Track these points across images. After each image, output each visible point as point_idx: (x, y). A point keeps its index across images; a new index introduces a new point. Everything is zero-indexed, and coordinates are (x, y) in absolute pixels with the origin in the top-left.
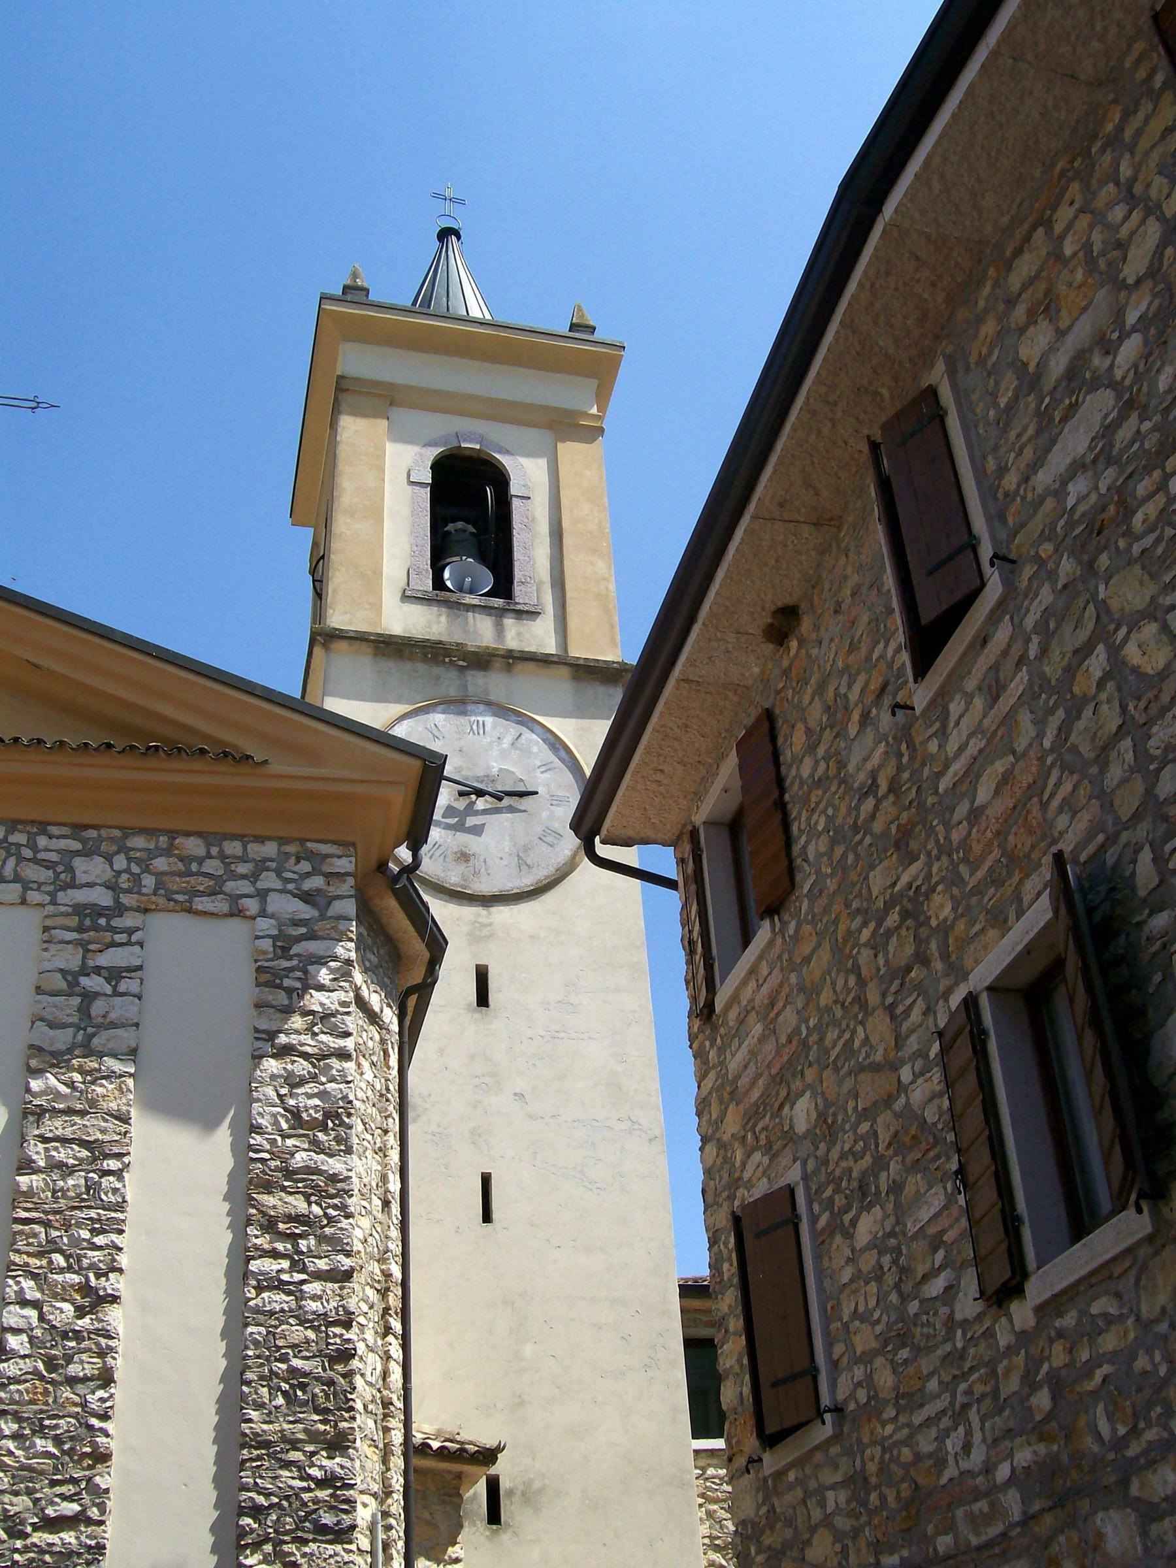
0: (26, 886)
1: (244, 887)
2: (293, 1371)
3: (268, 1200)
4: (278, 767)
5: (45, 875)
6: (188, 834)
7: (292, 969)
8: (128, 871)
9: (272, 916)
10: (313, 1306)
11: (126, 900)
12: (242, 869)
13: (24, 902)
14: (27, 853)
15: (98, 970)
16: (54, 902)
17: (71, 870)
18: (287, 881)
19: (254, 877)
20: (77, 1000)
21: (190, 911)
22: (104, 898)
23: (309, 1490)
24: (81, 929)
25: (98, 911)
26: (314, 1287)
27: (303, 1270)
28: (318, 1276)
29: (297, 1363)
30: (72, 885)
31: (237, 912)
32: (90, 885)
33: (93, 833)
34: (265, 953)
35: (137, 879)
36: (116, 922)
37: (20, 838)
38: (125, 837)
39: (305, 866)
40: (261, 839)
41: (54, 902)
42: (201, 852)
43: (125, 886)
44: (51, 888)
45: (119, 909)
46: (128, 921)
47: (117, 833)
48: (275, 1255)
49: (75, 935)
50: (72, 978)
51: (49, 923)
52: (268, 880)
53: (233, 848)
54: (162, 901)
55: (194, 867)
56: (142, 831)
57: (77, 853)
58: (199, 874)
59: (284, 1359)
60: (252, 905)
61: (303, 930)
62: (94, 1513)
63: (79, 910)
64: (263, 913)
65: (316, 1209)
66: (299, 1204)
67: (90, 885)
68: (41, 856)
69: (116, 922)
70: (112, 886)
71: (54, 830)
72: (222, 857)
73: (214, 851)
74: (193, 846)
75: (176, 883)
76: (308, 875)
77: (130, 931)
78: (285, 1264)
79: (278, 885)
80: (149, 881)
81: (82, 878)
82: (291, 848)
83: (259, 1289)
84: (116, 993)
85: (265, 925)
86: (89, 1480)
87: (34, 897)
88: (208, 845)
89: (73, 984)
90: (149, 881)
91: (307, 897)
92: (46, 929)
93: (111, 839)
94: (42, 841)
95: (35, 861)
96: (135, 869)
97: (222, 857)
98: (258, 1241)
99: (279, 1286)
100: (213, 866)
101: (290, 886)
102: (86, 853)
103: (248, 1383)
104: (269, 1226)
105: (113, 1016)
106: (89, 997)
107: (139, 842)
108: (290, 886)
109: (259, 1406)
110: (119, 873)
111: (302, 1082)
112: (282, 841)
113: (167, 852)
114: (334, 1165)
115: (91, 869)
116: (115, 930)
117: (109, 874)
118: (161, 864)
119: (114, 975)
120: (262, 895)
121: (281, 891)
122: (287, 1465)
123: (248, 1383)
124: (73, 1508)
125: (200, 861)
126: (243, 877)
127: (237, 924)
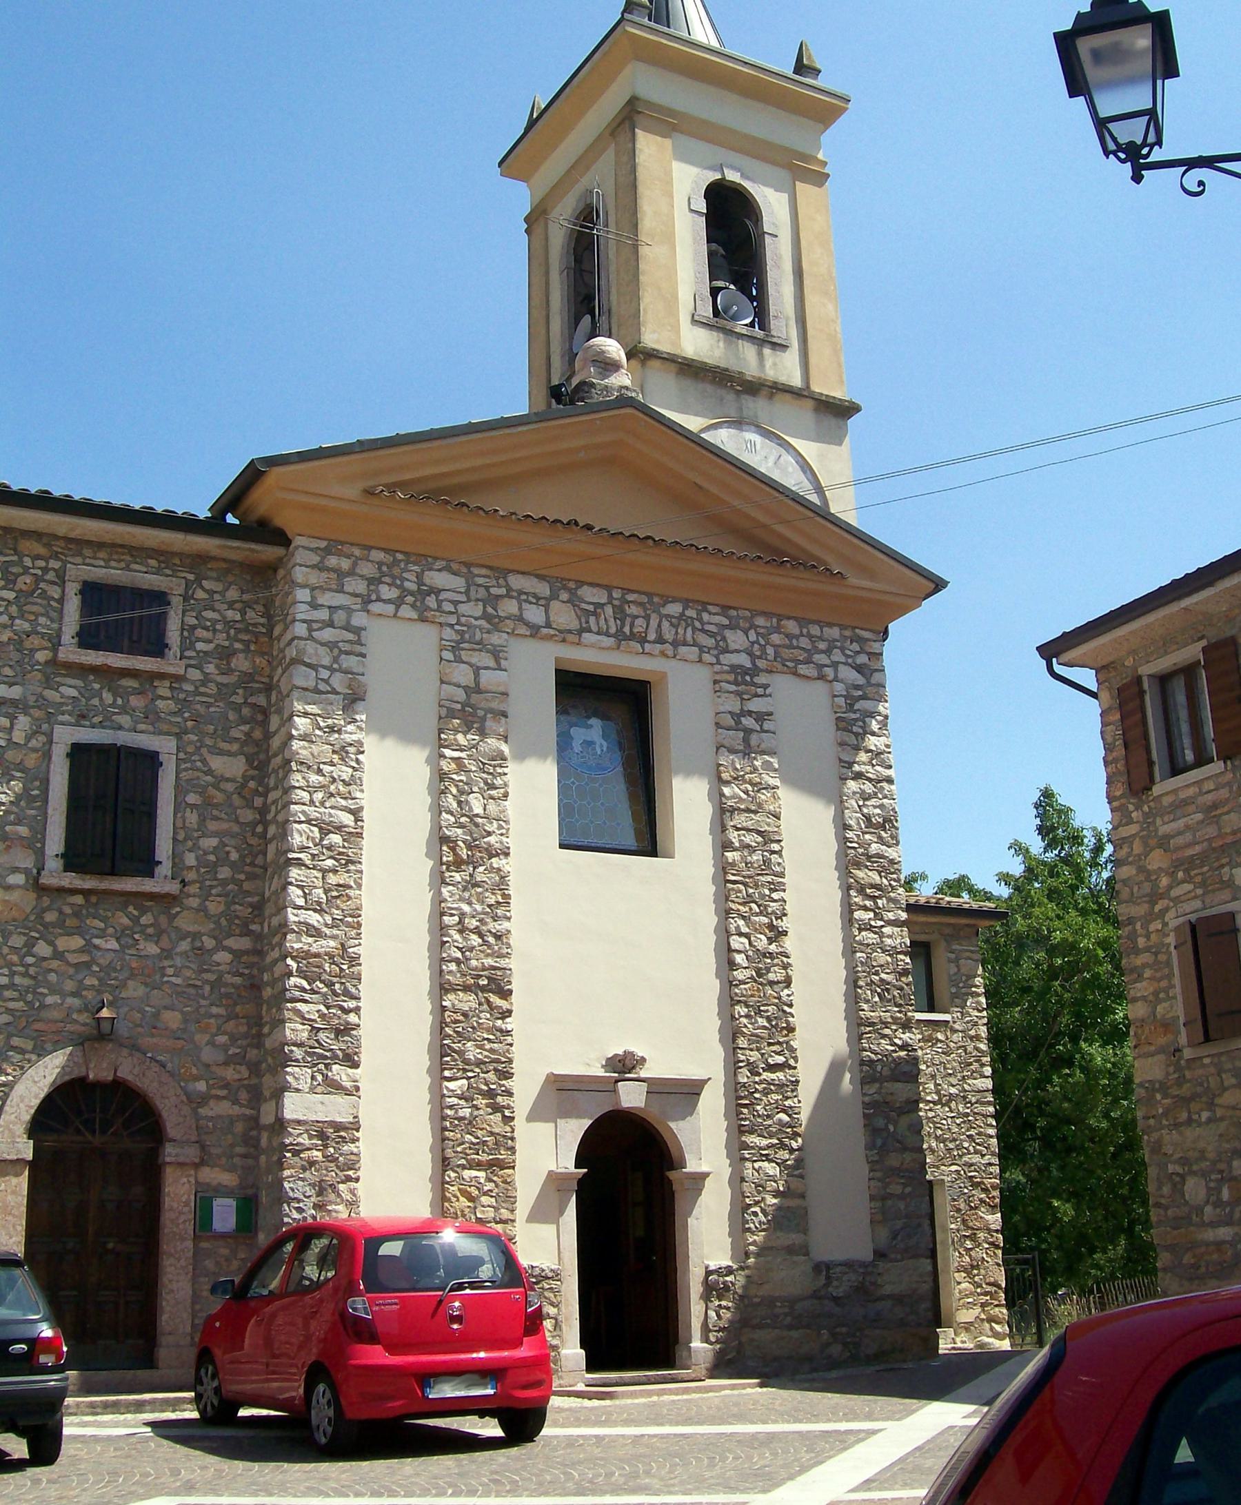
0: (701, 648)
1: (821, 659)
2: (882, 980)
3: (860, 874)
4: (853, 580)
5: (710, 642)
6: (789, 618)
7: (856, 720)
8: (757, 642)
9: (842, 681)
10: (888, 941)
11: (761, 664)
12: (822, 646)
13: (700, 661)
14: (697, 624)
15: (750, 713)
16: (719, 663)
17: (724, 639)
18: (848, 656)
19: (828, 652)
20: (741, 734)
21: (795, 674)
22: (744, 660)
23: (895, 1051)
24: (736, 683)
25: (746, 671)
26: (887, 930)
27: (881, 919)
28: (890, 923)
29: (883, 976)
30: (726, 651)
31: (821, 677)
32: (737, 651)
33: (733, 613)
34: (840, 707)
35: (763, 648)
36: (756, 680)
37: (691, 613)
38: (752, 617)
39: (855, 646)
40: (830, 625)
41: (719, 663)
42: (797, 631)
43: (758, 653)
44: (715, 652)
45: (755, 671)
46: (762, 679)
47: (748, 614)
48: (865, 908)
49: (733, 688)
50: (737, 717)
51: (718, 677)
52: (837, 656)
53: (815, 630)
54: (780, 667)
55: (795, 642)
56: (764, 614)
57: (725, 627)
58: (798, 647)
59: (877, 973)
60: (829, 672)
61: (860, 693)
62: (792, 1062)
63: (734, 668)
64: (836, 679)
65: (884, 880)
66: (875, 877)
67: (737, 651)
68: (707, 627)
69: (756, 680)
70: (750, 654)
71: (710, 608)
72: (810, 636)
73: (805, 631)
74: (791, 626)
75: (786, 653)
76: (858, 653)
77: (766, 686)
78: (871, 915)
79: (843, 659)
80: (770, 651)
81: (733, 646)
82: (847, 633)
83: (860, 930)
84: (763, 731)
85: (839, 688)
86: (787, 1043)
87: (707, 658)
88: (801, 627)
89: (738, 722)
90: (770, 651)
91: (859, 669)
92: (715, 682)
93: (744, 618)
94: (705, 616)
95: (703, 630)
96: (763, 642)
97: (810, 636)
98: (856, 900)
99: (870, 928)
100: (804, 642)
101: (850, 661)
102: (731, 627)
103: (860, 987)
104: (861, 891)
105: (763, 746)
106: (748, 731)
107: (760, 621)
108: (850, 661)
109: (867, 1001)
110: (753, 643)
111: (869, 798)
112: (842, 627)
113: (778, 629)
114: (891, 853)
115: (736, 639)
116: (755, 685)
117: (747, 644)
118: (776, 638)
119: (761, 717)
120: (835, 665)
121: (845, 664)
122: (884, 1036)
123: (860, 987)
124: (780, 1059)
125: (797, 637)
126: (822, 652)
127: (820, 683)
